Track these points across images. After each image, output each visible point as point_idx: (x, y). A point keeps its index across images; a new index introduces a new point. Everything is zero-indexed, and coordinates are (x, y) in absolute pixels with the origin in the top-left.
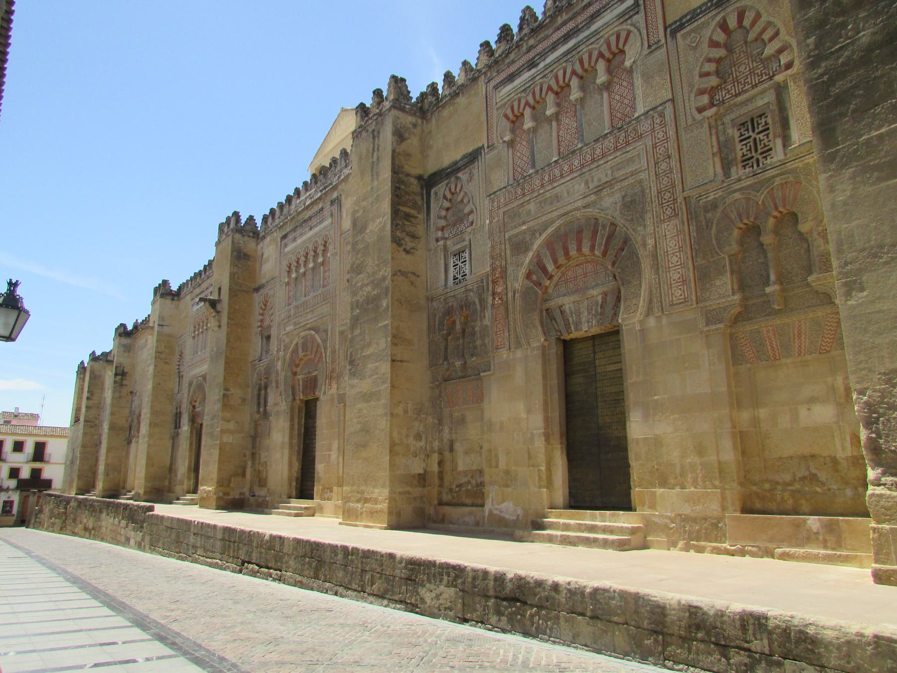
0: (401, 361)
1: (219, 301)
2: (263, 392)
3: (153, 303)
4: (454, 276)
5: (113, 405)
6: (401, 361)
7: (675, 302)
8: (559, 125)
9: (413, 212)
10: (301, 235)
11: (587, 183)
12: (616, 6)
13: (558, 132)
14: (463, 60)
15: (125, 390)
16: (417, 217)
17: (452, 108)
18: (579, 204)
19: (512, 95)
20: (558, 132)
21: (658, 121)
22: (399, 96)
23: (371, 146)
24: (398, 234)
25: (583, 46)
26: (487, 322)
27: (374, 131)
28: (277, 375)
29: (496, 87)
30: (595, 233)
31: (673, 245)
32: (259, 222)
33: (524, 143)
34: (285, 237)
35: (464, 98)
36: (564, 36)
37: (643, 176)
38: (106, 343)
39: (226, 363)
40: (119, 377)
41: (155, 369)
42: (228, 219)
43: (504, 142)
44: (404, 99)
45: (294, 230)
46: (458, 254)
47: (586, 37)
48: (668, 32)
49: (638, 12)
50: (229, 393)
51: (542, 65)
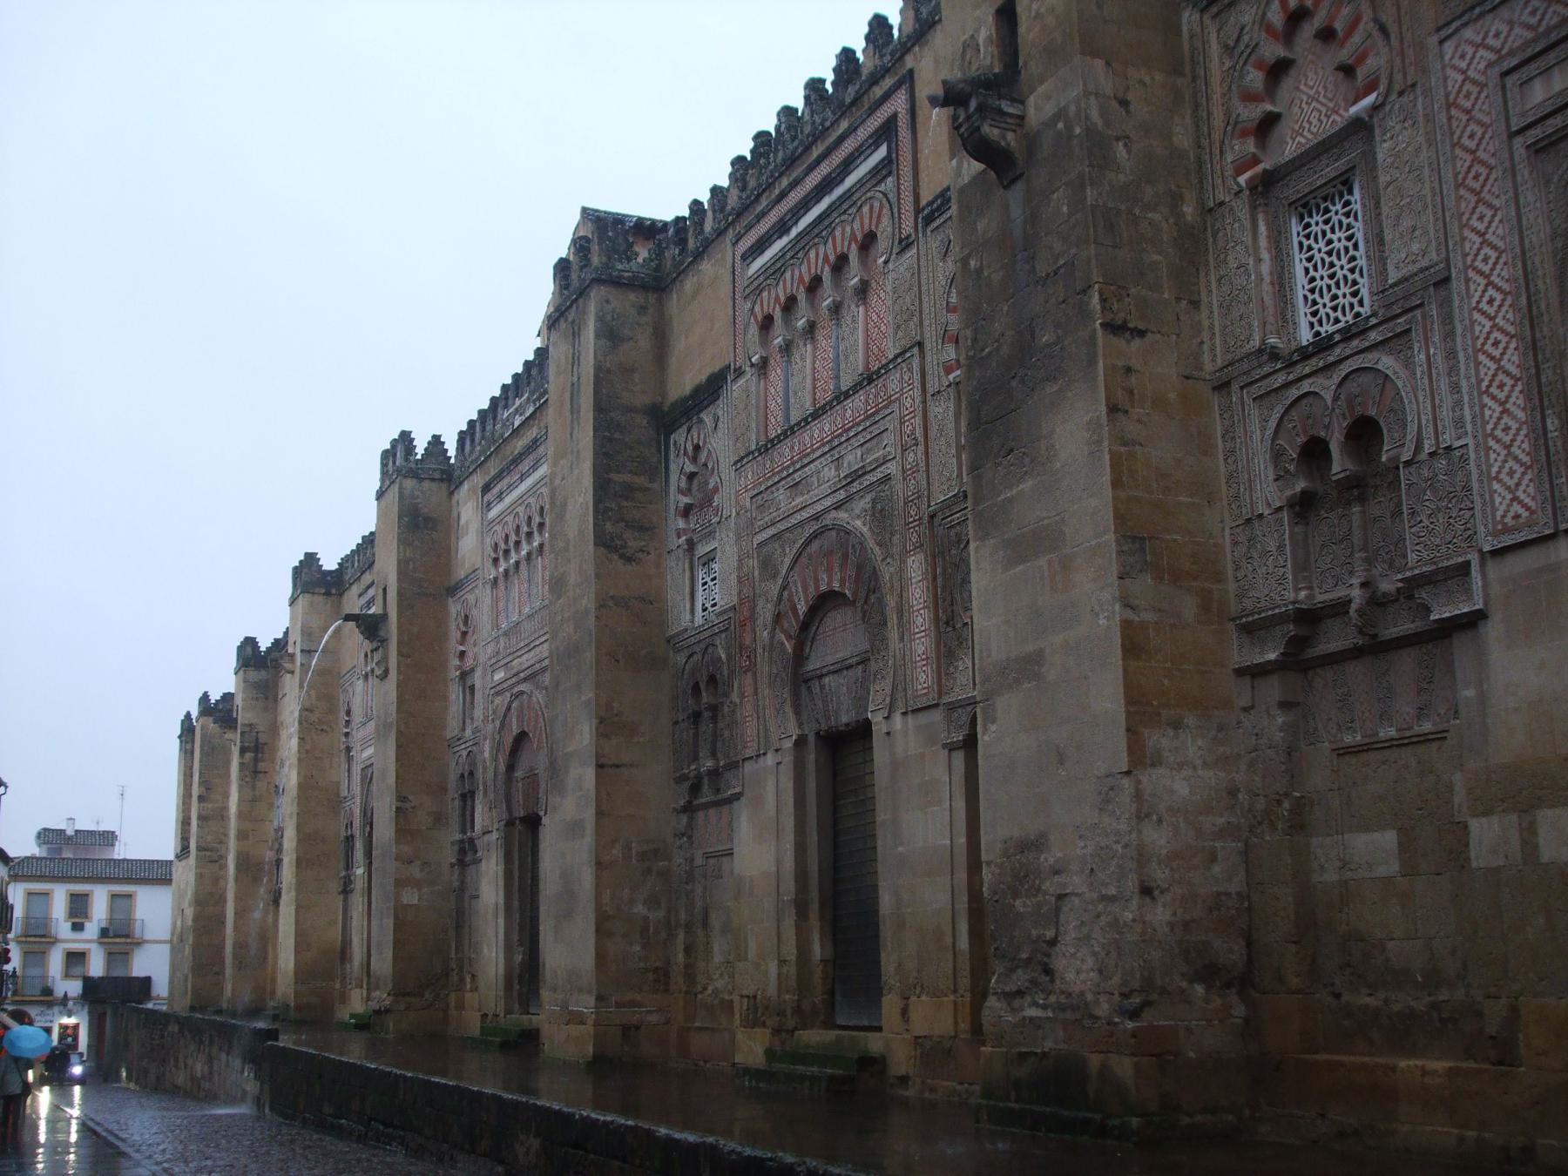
0: (618, 766)
1: (384, 617)
2: (469, 803)
3: (293, 601)
4: (703, 605)
5: (241, 815)
6: (618, 766)
7: (919, 693)
8: (815, 348)
9: (641, 480)
10: (511, 487)
11: (837, 469)
12: (868, 152)
13: (814, 363)
14: (711, 186)
15: (261, 785)
16: (648, 489)
17: (696, 278)
18: (828, 502)
19: (762, 278)
20: (814, 363)
21: (906, 378)
22: (609, 258)
23: (571, 351)
24: (609, 527)
25: (835, 214)
26: (735, 698)
27: (573, 322)
28: (485, 768)
29: (744, 257)
30: (845, 556)
31: (918, 596)
32: (451, 448)
33: (779, 371)
34: (486, 488)
35: (709, 266)
36: (816, 187)
37: (892, 468)
38: (223, 680)
39: (399, 747)
40: (249, 756)
41: (300, 746)
42: (394, 443)
43: (752, 365)
44: (620, 261)
45: (499, 477)
46: (709, 559)
47: (841, 197)
48: (920, 220)
49: (890, 173)
50: (408, 805)
51: (794, 232)
